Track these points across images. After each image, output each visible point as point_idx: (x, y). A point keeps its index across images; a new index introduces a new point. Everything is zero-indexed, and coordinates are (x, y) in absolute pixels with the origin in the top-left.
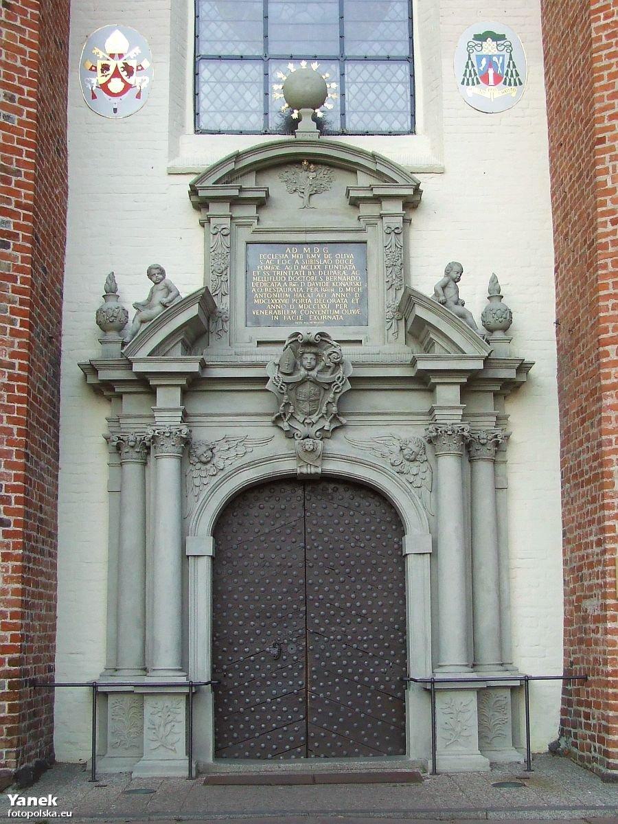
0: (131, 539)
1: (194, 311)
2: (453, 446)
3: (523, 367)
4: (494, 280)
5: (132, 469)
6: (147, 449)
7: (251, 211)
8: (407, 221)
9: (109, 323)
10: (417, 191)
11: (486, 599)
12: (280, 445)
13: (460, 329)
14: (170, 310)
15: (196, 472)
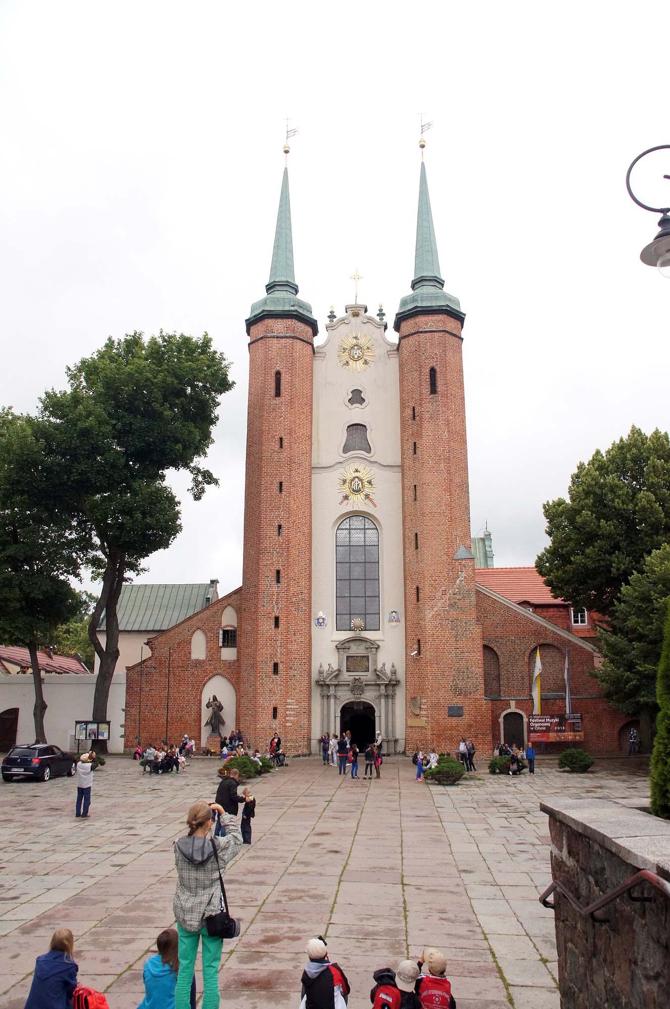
0: (325, 712)
1: (337, 672)
2: (383, 697)
3: (399, 681)
4: (393, 664)
5: (325, 700)
6: (328, 697)
7: (347, 650)
8: (376, 651)
9: (320, 673)
10: (379, 646)
11: (390, 725)
12: (352, 696)
13: (384, 675)
14: (332, 672)
15: (337, 701)
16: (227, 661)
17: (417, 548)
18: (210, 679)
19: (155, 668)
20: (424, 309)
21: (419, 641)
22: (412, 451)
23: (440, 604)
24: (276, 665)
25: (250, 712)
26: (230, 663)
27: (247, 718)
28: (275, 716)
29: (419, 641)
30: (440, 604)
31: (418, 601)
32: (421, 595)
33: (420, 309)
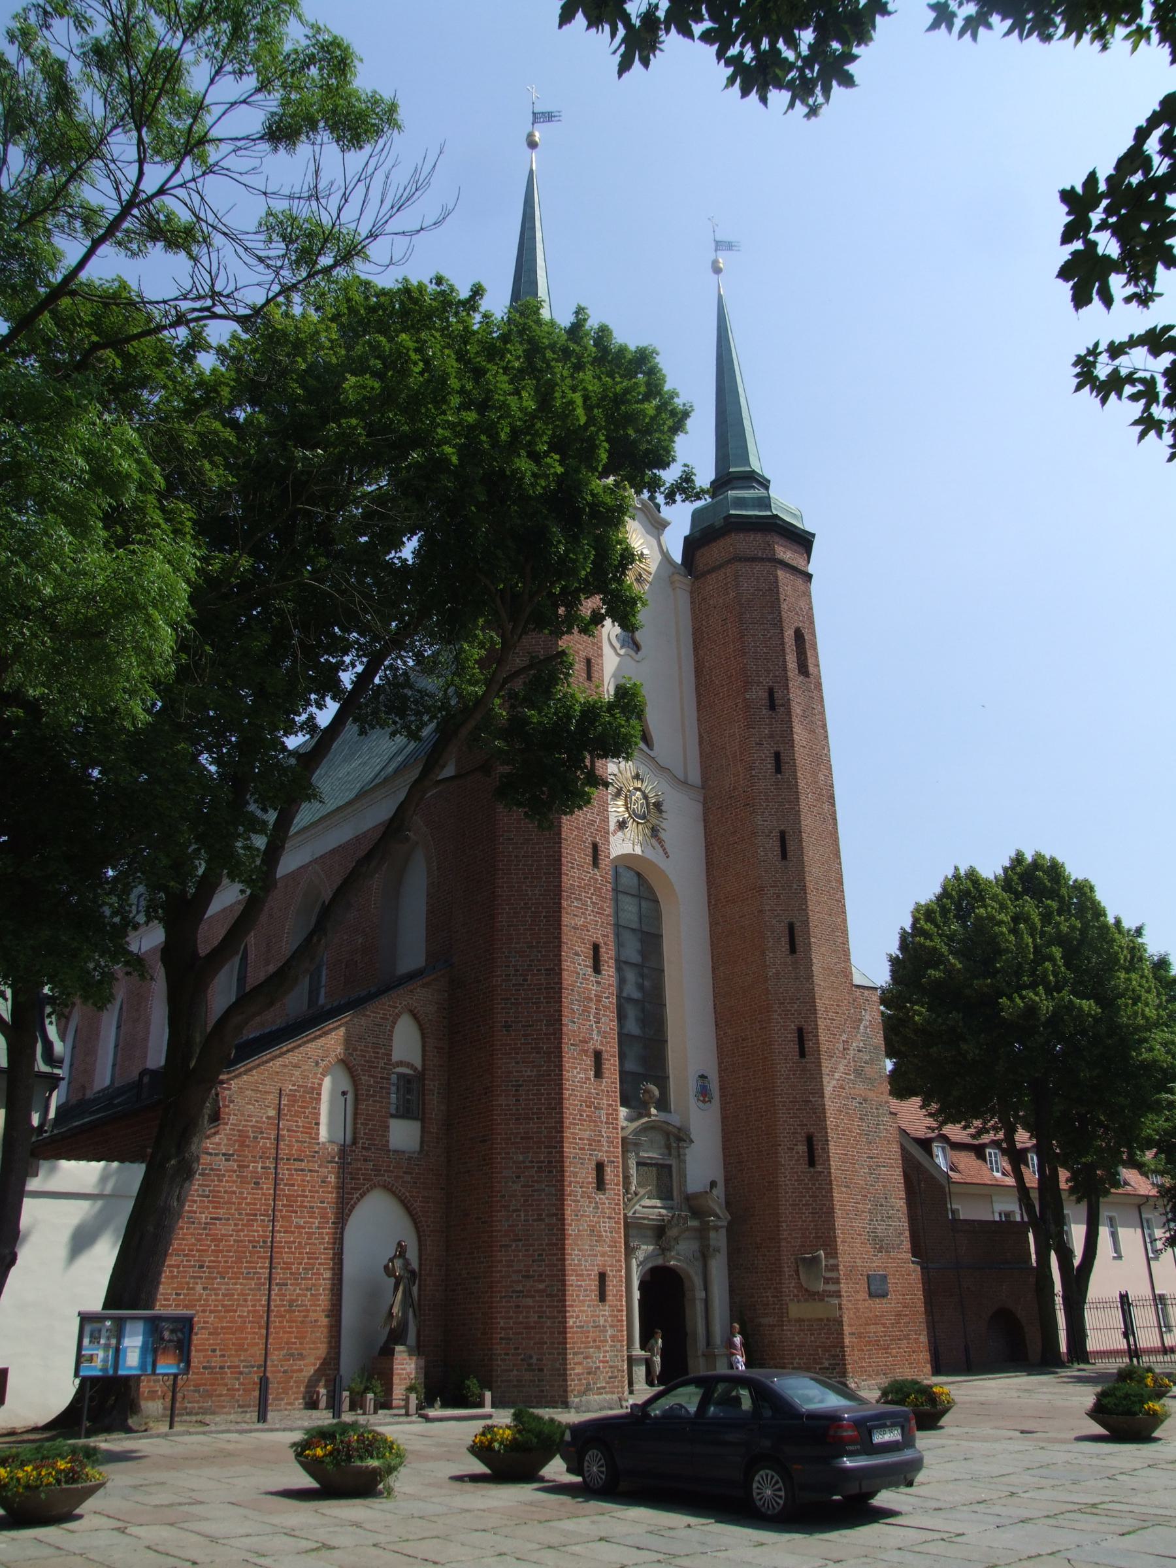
16: (404, 1152)
17: (793, 950)
18: (362, 1196)
19: (228, 1157)
20: (785, 525)
21: (810, 1140)
22: (770, 765)
23: (841, 1068)
24: (600, 1168)
25: (542, 1286)
26: (410, 1159)
27: (529, 1302)
28: (602, 1297)
29: (810, 1140)
30: (841, 1068)
31: (802, 1054)
32: (809, 1044)
33: (781, 523)
